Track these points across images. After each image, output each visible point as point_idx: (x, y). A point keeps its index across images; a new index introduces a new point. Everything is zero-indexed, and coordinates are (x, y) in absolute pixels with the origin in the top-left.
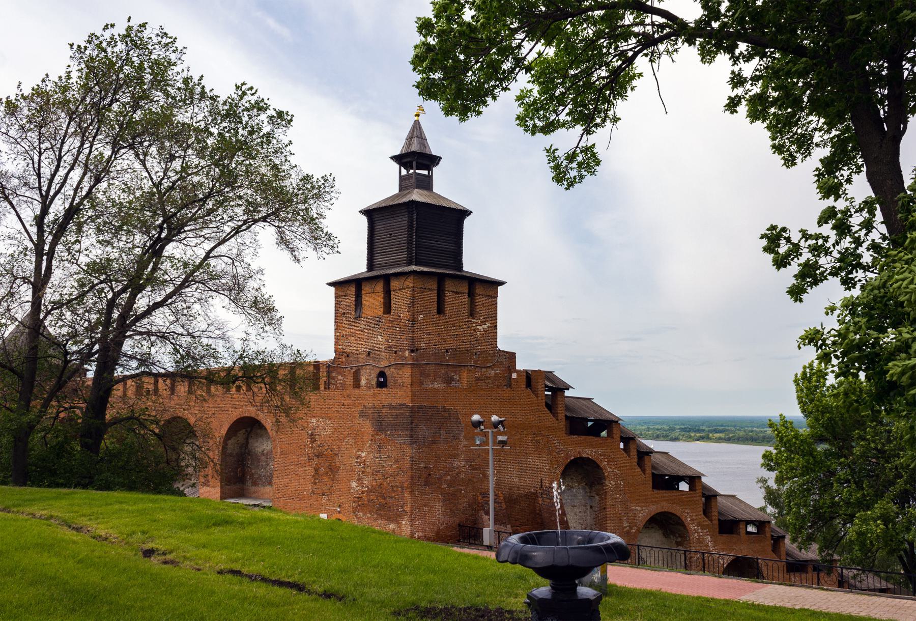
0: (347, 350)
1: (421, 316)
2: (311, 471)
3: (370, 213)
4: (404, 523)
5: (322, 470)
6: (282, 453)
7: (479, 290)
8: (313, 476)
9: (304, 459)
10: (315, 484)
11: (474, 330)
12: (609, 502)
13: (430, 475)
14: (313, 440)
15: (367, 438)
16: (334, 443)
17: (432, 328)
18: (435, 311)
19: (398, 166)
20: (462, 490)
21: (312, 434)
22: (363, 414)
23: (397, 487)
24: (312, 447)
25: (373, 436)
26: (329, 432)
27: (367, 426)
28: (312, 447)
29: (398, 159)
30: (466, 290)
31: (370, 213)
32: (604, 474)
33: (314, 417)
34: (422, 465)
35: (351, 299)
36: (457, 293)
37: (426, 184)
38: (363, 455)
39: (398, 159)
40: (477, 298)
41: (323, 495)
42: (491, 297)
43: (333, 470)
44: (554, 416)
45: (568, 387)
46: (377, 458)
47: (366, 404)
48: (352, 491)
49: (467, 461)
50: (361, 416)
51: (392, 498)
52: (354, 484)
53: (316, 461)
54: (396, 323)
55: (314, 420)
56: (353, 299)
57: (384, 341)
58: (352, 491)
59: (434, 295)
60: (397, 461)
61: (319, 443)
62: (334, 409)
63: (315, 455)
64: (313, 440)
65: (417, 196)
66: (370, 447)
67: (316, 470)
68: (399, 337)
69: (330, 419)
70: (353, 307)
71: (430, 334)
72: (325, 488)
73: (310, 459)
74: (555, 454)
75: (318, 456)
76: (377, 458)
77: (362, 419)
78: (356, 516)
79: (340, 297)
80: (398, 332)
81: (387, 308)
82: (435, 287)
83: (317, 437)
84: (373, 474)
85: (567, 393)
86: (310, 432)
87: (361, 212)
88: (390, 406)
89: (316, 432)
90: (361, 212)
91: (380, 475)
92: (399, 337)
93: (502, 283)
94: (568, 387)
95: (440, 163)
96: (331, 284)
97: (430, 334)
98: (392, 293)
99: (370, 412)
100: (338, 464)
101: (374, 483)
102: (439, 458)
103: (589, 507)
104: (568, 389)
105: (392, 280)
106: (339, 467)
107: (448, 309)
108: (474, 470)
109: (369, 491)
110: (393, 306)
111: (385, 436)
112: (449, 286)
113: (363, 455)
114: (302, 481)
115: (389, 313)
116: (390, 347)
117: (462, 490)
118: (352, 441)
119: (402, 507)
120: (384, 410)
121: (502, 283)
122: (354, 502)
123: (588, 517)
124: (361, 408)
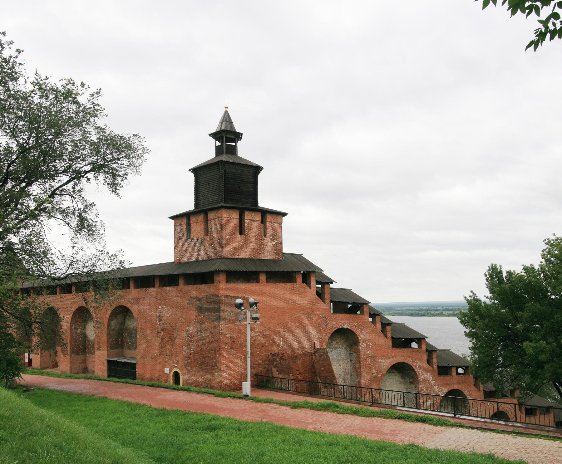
1: (228, 236)
2: (159, 340)
3: (196, 171)
4: (216, 374)
6: (141, 329)
7: (269, 218)
8: (160, 344)
9: (155, 332)
10: (162, 348)
11: (266, 245)
12: (362, 357)
13: (234, 342)
14: (160, 320)
16: (172, 322)
17: (235, 245)
18: (238, 233)
19: (214, 140)
20: (257, 351)
21: (159, 316)
22: (190, 302)
23: (212, 350)
25: (196, 316)
27: (193, 310)
28: (159, 325)
29: (214, 135)
30: (260, 219)
31: (196, 171)
32: (358, 338)
33: (160, 305)
34: (228, 335)
35: (184, 227)
36: (254, 221)
37: (233, 151)
39: (214, 135)
40: (267, 224)
41: (167, 355)
42: (278, 223)
43: (172, 339)
44: (323, 301)
45: (332, 282)
47: (192, 295)
49: (261, 332)
51: (208, 357)
52: (185, 348)
53: (162, 333)
54: (212, 241)
55: (160, 307)
56: (185, 227)
57: (204, 253)
59: (237, 222)
60: (211, 333)
63: (162, 330)
64: (160, 320)
65: (225, 158)
66: (194, 324)
67: (162, 339)
68: (214, 251)
69: (170, 306)
70: (185, 232)
71: (234, 248)
73: (158, 332)
74: (324, 326)
76: (199, 331)
78: (187, 369)
79: (177, 226)
80: (213, 248)
81: (207, 232)
82: (238, 217)
84: (197, 342)
85: (332, 286)
86: (158, 315)
87: (190, 170)
88: (207, 297)
89: (162, 315)
90: (190, 170)
92: (214, 251)
93: (284, 214)
94: (332, 282)
95: (243, 137)
96: (172, 218)
97: (234, 248)
98: (209, 222)
99: (194, 301)
100: (175, 336)
101: (198, 348)
102: (240, 331)
103: (349, 361)
104: (332, 283)
105: (209, 213)
106: (176, 337)
107: (247, 230)
108: (266, 338)
109: (195, 353)
110: (210, 230)
111: (204, 316)
112: (248, 216)
115: (208, 235)
117: (257, 351)
118: (183, 320)
119: (215, 363)
121: (284, 214)
123: (349, 367)
124: (188, 298)
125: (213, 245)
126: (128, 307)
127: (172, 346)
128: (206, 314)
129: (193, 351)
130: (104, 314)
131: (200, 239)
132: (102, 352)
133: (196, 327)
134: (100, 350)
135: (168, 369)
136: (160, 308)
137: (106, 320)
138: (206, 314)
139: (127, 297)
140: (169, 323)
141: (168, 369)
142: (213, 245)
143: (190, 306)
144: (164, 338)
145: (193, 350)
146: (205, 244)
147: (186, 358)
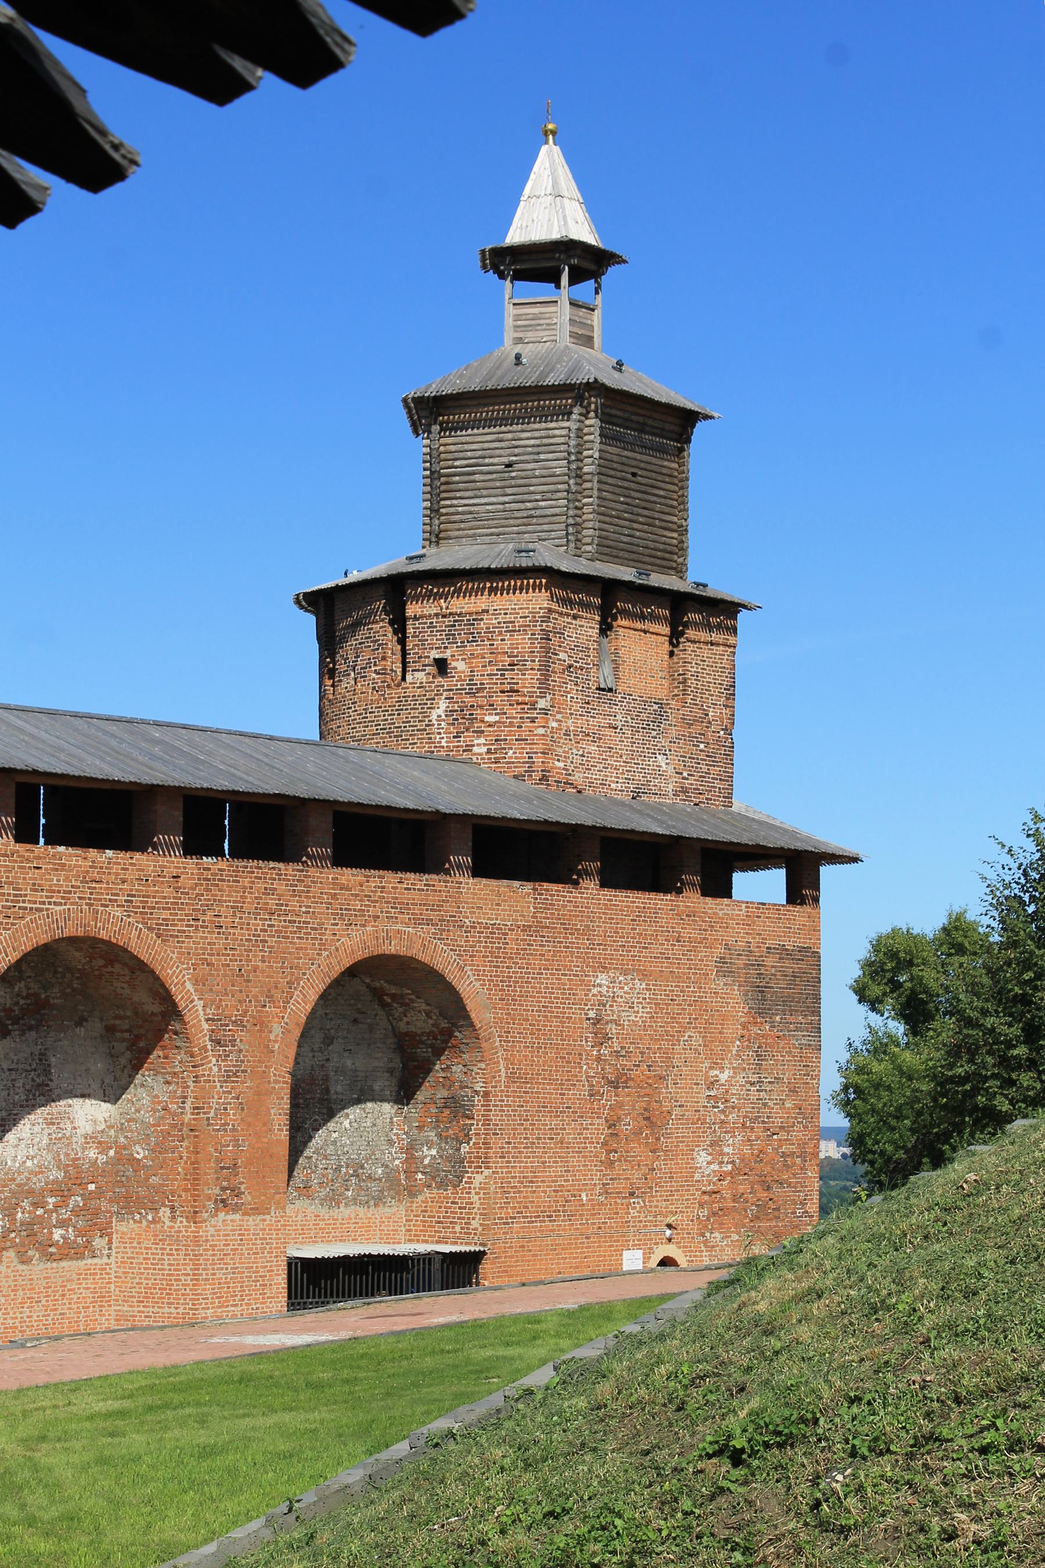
0: (578, 778)
2: (598, 1127)
5: (627, 1125)
6: (512, 1078)
8: (605, 1144)
14: (602, 1039)
15: (733, 1030)
21: (597, 1021)
24: (598, 1059)
25: (744, 1026)
26: (641, 1014)
28: (598, 1059)
33: (605, 969)
38: (724, 1077)
41: (632, 1194)
43: (652, 1119)
46: (752, 1084)
48: (697, 1177)
50: (722, 973)
52: (702, 1158)
53: (609, 1099)
54: (695, 729)
55: (602, 979)
57: (670, 770)
58: (697, 1177)
60: (793, 1091)
61: (617, 1047)
62: (656, 949)
64: (602, 1039)
68: (705, 768)
69: (644, 975)
72: (636, 1175)
75: (614, 1084)
76: (752, 1084)
77: (721, 982)
78: (705, 1242)
83: (612, 1029)
86: (592, 1014)
89: (609, 1014)
91: (759, 1131)
92: (705, 768)
99: (741, 963)
100: (666, 1105)
113: (724, 1077)
114: (574, 1161)
116: (685, 790)
118: (697, 1041)
120: (770, 961)
122: (701, 1205)
124: (720, 950)
125: (702, 746)
126: (439, 967)
127: (653, 1151)
128: (778, 1018)
129: (730, 1167)
130: (277, 995)
131: (656, 707)
132: (251, 1221)
133: (744, 1069)
134: (236, 1208)
135: (639, 1254)
136: (600, 985)
137: (286, 1031)
138: (778, 1018)
139: (434, 916)
140: (642, 1053)
141: (639, 1254)
142: (702, 746)
143: (726, 985)
144: (619, 1119)
145: (733, 1162)
146: (673, 732)
147: (706, 1198)
